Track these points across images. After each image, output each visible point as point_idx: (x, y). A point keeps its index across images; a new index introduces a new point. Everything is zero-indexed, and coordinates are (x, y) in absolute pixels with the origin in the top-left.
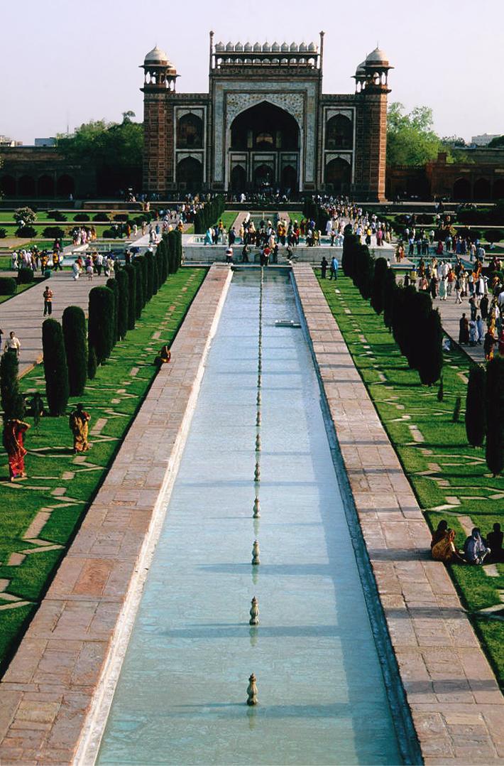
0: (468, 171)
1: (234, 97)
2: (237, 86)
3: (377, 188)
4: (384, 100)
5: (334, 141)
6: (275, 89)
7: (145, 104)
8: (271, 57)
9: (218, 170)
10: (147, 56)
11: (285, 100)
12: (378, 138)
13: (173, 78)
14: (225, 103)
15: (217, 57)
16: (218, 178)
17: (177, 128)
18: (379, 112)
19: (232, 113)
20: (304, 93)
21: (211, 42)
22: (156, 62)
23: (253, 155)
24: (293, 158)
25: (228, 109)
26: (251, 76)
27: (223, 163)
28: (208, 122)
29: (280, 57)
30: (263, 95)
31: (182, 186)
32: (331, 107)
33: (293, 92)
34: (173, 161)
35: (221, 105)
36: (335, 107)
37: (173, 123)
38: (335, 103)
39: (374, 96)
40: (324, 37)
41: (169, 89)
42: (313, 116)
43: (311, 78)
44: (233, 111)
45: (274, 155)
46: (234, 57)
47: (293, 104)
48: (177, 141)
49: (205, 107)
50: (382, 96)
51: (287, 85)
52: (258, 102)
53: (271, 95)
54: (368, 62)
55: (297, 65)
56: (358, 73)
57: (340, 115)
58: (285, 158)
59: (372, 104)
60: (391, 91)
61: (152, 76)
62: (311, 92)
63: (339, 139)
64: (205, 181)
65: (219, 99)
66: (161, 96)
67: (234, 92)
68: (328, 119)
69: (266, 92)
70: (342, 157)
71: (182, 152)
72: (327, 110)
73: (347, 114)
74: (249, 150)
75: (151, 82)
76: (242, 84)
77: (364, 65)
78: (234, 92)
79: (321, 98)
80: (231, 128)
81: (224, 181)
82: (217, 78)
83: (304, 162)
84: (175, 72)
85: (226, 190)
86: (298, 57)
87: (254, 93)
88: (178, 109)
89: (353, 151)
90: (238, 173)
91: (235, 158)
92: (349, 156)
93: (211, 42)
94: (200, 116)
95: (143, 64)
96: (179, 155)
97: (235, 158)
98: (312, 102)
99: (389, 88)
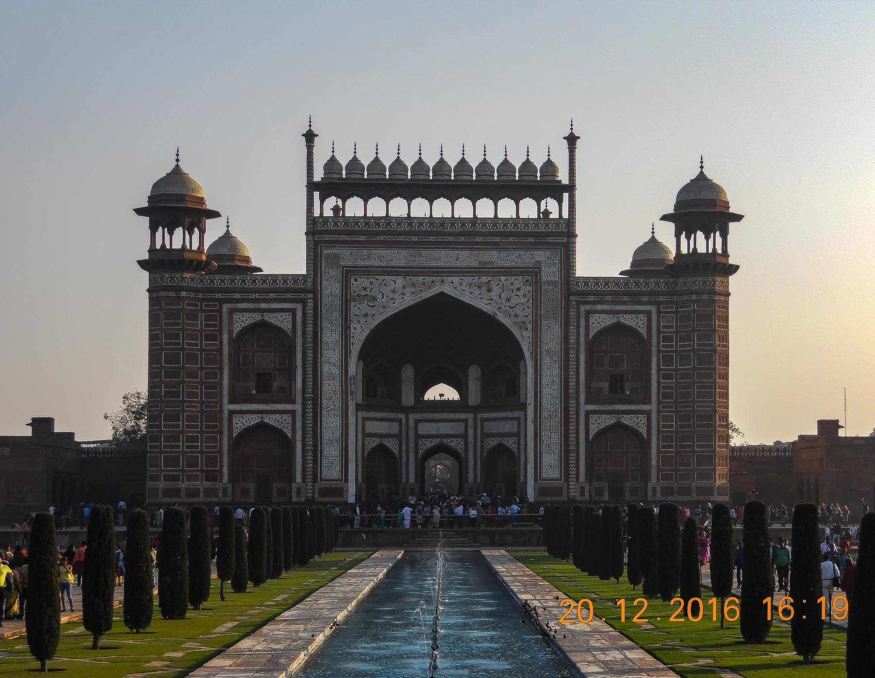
1: (366, 283)
4: (722, 289)
6: (464, 264)
11: (489, 290)
14: (346, 300)
17: (230, 355)
19: (363, 320)
20: (533, 273)
25: (354, 310)
28: (304, 342)
30: (435, 278)
32: (599, 307)
33: (509, 272)
34: (221, 433)
35: (338, 302)
36: (605, 307)
38: (609, 298)
40: (579, 143)
43: (550, 240)
44: (366, 315)
47: (508, 300)
51: (494, 257)
52: (426, 295)
53: (456, 280)
54: (678, 205)
57: (618, 329)
59: (694, 297)
60: (737, 267)
62: (550, 273)
63: (617, 383)
65: (331, 287)
67: (367, 271)
68: (591, 334)
72: (588, 313)
73: (637, 322)
78: (367, 271)
79: (574, 288)
80: (362, 356)
82: (327, 238)
87: (416, 274)
90: (380, 463)
94: (287, 326)
96: (235, 419)
99: (731, 261)
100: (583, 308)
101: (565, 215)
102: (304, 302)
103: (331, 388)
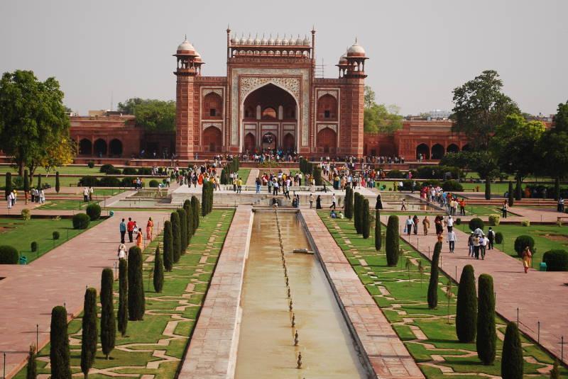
0: (427, 138)
2: (249, 71)
3: (357, 151)
5: (323, 114)
7: (177, 85)
8: (274, 49)
9: (234, 136)
10: (180, 47)
12: (358, 112)
13: (199, 65)
15: (233, 49)
16: (234, 143)
18: (358, 92)
20: (299, 78)
21: (228, 38)
22: (188, 52)
23: (262, 125)
24: (292, 127)
26: (260, 63)
27: (237, 131)
28: (226, 99)
29: (281, 49)
31: (206, 149)
33: (292, 77)
35: (236, 86)
37: (199, 99)
39: (354, 80)
41: (196, 73)
42: (308, 95)
45: (278, 125)
46: (246, 49)
48: (203, 115)
49: (224, 88)
50: (360, 80)
51: (287, 72)
52: (265, 84)
53: (275, 79)
54: (349, 54)
55: (295, 56)
56: (340, 62)
57: (328, 95)
58: (286, 127)
61: (182, 63)
63: (327, 114)
64: (224, 144)
65: (234, 81)
66: (191, 79)
67: (247, 76)
69: (271, 77)
70: (330, 126)
71: (206, 122)
72: (318, 90)
74: (258, 121)
75: (182, 68)
76: (253, 70)
77: (346, 56)
78: (247, 76)
81: (239, 145)
83: (301, 131)
84: (200, 60)
85: (241, 151)
86: (295, 50)
88: (203, 89)
89: (339, 122)
91: (247, 127)
92: (335, 126)
93: (228, 38)
95: (176, 53)
97: (247, 127)
98: (306, 85)
99: (365, 74)
100: (316, 89)
101: (311, 57)
102: (226, 86)
103: (234, 115)
